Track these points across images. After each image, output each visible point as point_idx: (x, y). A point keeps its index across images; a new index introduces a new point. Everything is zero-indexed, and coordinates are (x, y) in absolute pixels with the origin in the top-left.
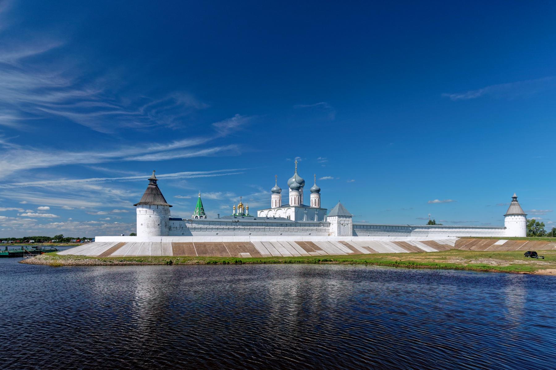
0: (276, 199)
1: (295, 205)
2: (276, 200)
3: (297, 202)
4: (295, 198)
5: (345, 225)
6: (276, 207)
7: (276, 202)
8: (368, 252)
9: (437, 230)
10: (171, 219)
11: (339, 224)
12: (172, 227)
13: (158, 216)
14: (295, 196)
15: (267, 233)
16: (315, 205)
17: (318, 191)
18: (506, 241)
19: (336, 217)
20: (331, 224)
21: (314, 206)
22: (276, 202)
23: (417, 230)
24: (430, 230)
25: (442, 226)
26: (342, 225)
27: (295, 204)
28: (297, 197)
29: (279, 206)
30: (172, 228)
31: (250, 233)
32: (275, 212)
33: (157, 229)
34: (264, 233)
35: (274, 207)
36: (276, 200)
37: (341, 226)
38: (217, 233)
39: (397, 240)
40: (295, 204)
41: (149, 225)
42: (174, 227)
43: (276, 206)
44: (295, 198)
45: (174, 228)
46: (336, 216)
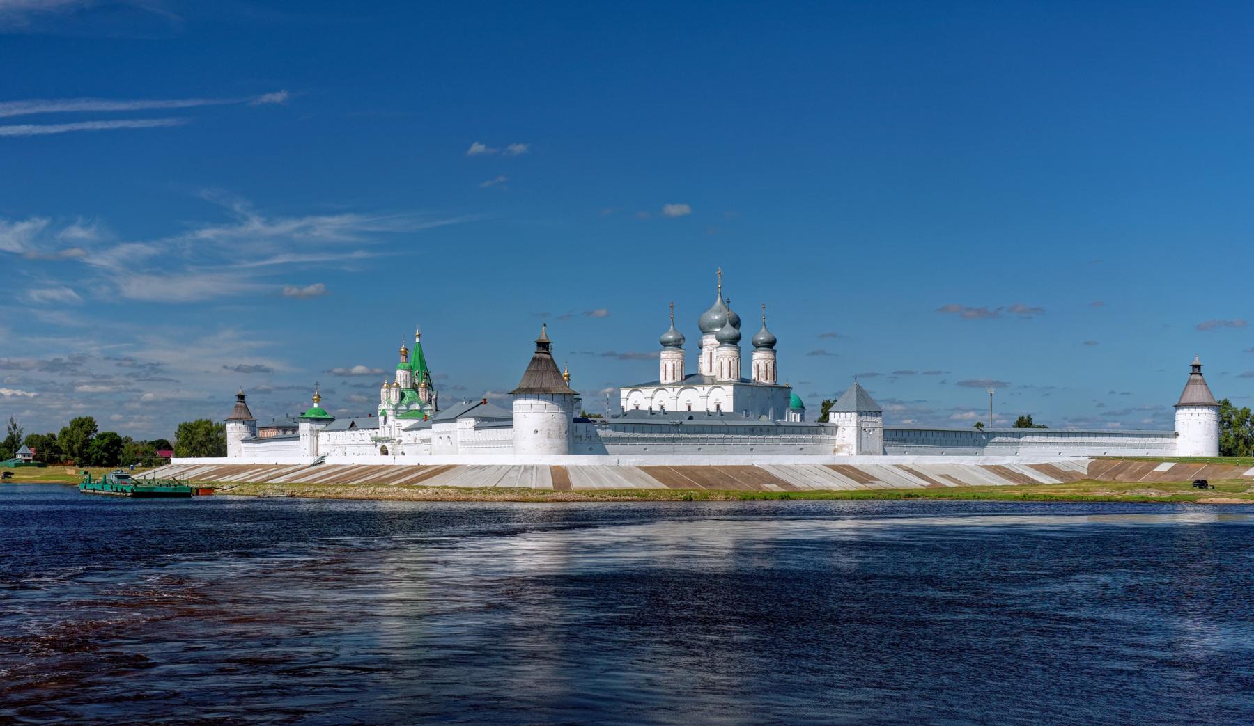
0: (675, 362)
1: (731, 379)
2: (674, 365)
4: (730, 362)
5: (870, 431)
6: (675, 381)
8: (955, 485)
9: (1036, 439)
11: (860, 429)
13: (565, 416)
14: (731, 359)
15: (727, 447)
16: (767, 379)
17: (770, 345)
18: (1172, 465)
19: (853, 413)
20: (840, 429)
21: (762, 380)
23: (997, 439)
24: (1022, 440)
25: (1048, 430)
27: (730, 377)
28: (736, 360)
31: (699, 446)
32: (675, 394)
33: (564, 440)
34: (723, 448)
35: (670, 380)
37: (863, 431)
38: (645, 447)
39: (988, 463)
40: (730, 377)
41: (551, 432)
43: (674, 379)
44: (730, 362)
46: (853, 411)
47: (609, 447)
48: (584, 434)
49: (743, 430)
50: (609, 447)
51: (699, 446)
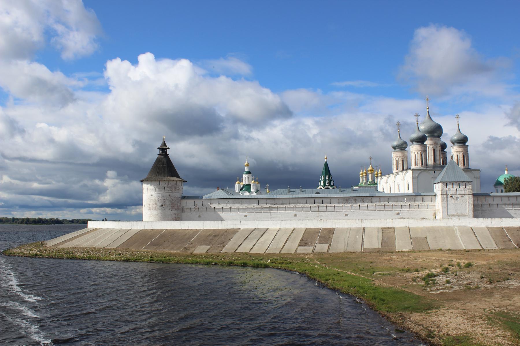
0: (397, 159)
1: (416, 166)
2: (397, 161)
3: (419, 161)
4: (416, 155)
5: (457, 198)
6: (398, 171)
7: (397, 163)
10: (184, 198)
11: (445, 196)
12: (185, 207)
13: (160, 195)
14: (416, 153)
22: (397, 163)
26: (451, 197)
28: (419, 153)
29: (402, 169)
30: (186, 210)
31: (295, 213)
33: (159, 212)
34: (318, 214)
36: (397, 161)
37: (449, 199)
38: (245, 214)
40: (416, 165)
41: (150, 206)
42: (187, 209)
44: (416, 155)
45: (188, 210)
47: (223, 215)
48: (193, 207)
49: (312, 200)
50: (223, 215)
51: (295, 213)
